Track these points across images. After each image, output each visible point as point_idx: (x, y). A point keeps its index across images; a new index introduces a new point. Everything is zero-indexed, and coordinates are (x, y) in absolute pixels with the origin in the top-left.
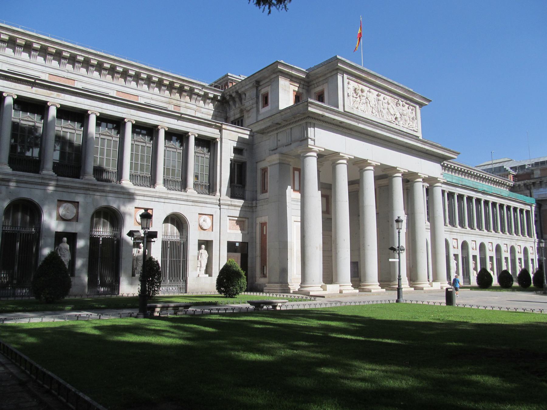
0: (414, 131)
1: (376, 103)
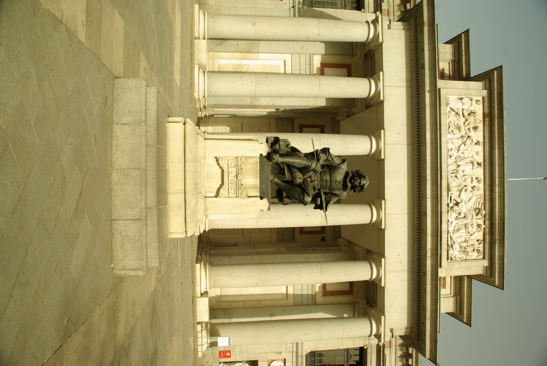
0: (448, 251)
1: (468, 160)
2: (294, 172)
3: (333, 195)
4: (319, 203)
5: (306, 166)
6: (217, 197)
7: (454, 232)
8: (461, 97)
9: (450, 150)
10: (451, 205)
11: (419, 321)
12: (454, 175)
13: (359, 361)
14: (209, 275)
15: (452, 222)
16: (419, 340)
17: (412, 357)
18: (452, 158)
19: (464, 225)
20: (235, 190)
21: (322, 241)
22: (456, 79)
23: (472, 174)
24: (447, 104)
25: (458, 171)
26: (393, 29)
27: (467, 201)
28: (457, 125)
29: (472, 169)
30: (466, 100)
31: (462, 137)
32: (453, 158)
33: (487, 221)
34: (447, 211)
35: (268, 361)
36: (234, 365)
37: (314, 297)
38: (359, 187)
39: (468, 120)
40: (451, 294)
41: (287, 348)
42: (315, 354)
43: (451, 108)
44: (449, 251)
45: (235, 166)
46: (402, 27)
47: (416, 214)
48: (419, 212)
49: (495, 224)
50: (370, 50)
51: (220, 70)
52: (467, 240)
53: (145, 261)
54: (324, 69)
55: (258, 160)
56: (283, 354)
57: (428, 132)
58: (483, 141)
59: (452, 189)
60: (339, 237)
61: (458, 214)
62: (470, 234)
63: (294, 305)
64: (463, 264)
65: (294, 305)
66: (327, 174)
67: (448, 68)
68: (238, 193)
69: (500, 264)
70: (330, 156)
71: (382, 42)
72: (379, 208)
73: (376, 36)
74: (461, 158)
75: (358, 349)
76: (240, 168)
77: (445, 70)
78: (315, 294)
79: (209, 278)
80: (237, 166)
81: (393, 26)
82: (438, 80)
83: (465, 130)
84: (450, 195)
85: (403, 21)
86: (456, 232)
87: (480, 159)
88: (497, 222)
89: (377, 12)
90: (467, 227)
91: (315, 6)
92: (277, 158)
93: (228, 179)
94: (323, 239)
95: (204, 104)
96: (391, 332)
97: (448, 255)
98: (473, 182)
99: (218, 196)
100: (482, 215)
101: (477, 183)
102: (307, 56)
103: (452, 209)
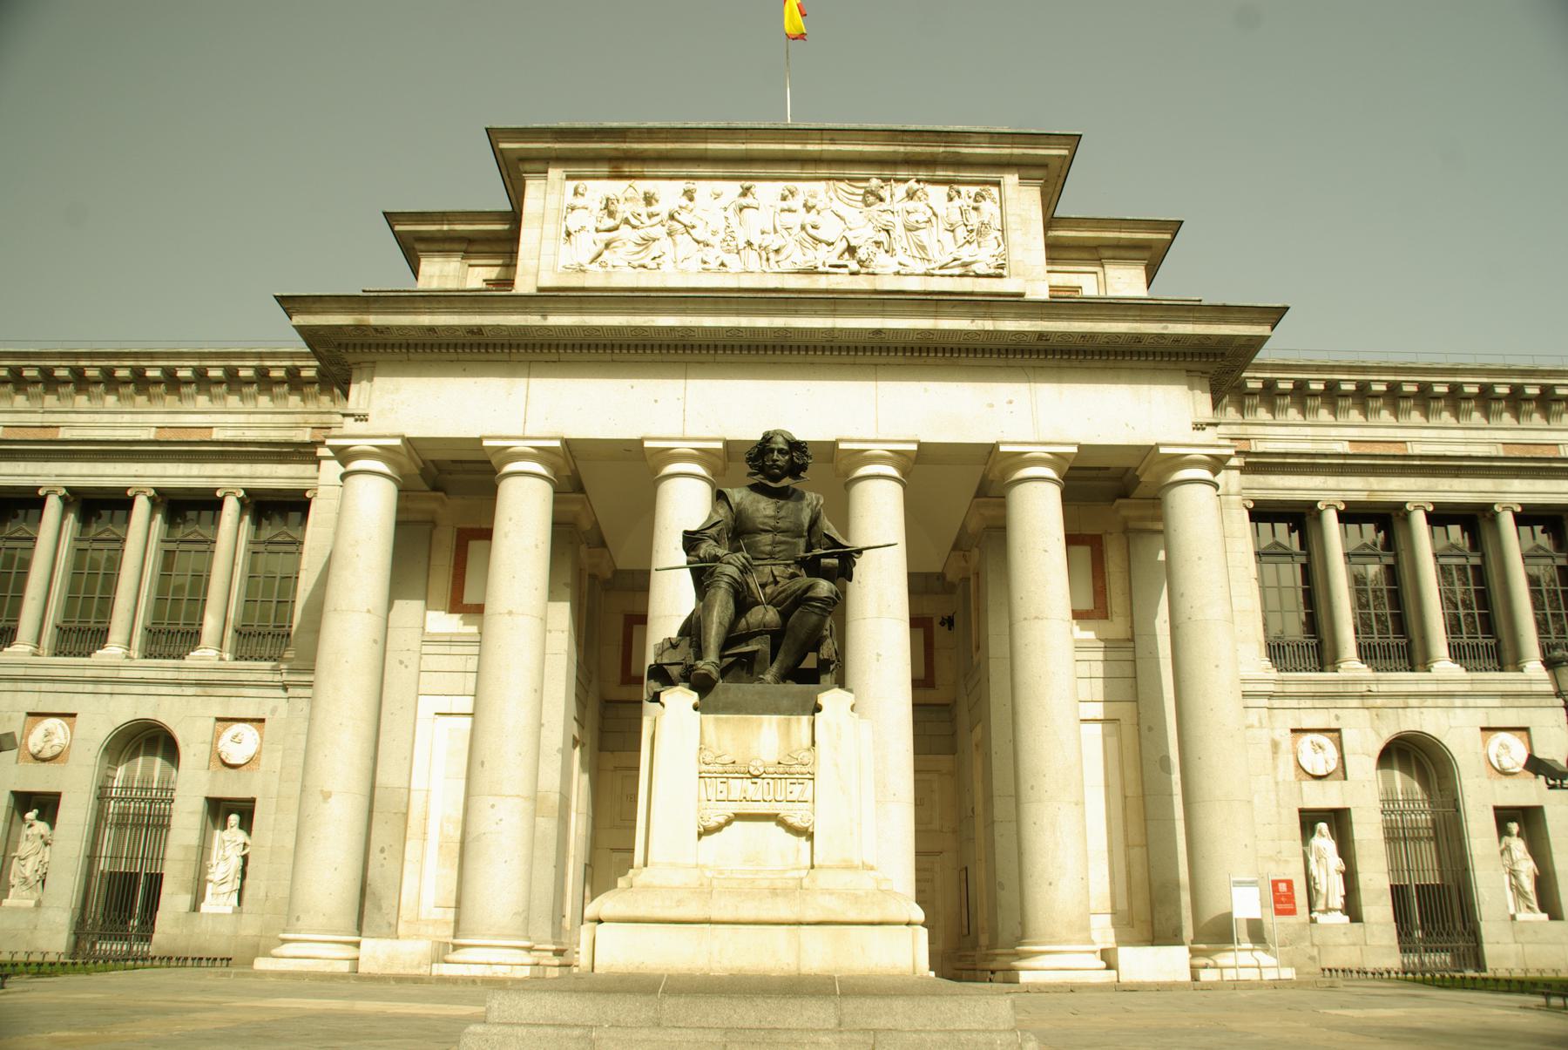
0: (978, 276)
1: (734, 221)
2: (748, 628)
3: (815, 528)
4: (836, 561)
5: (732, 590)
6: (813, 833)
7: (928, 260)
8: (564, 235)
9: (706, 266)
10: (854, 266)
11: (1170, 354)
12: (772, 255)
13: (1291, 524)
14: (1050, 943)
15: (901, 264)
16: (1223, 354)
17: (1273, 382)
19: (909, 233)
20: (795, 784)
21: (953, 625)
22: (515, 250)
23: (772, 210)
24: (580, 270)
25: (764, 245)
26: (368, 407)
27: (845, 223)
28: (639, 245)
29: (757, 209)
30: (573, 222)
31: (670, 234)
32: (727, 259)
33: (898, 173)
35: (1300, 780)
36: (1317, 881)
37: (1110, 645)
38: (794, 454)
39: (626, 218)
40: (1096, 273)
41: (1261, 722)
42: (1274, 647)
43: (592, 261)
44: (978, 272)
45: (725, 780)
46: (364, 384)
47: (877, 358)
48: (872, 349)
49: (906, 153)
50: (420, 475)
51: (453, 904)
52: (948, 227)
53: (994, 1036)
54: (467, 605)
55: (711, 717)
56: (1277, 738)
57: (653, 321)
58: (685, 181)
59: (812, 264)
60: (941, 576)
61: (879, 247)
62: (933, 218)
63: (1135, 699)
64: (1013, 236)
65: (1135, 699)
66: (754, 542)
67: (484, 268)
68: (802, 774)
69: (1013, 144)
70: (706, 531)
71: (402, 437)
72: (860, 457)
73: (385, 453)
74: (729, 238)
75: (1257, 526)
76: (730, 768)
77: (488, 277)
78: (1101, 640)
79: (1059, 943)
80: (725, 775)
81: (361, 407)
82: (513, 292)
83: (651, 226)
84: (827, 269)
85: (349, 383)
86: (926, 254)
88: (902, 149)
89: (318, 454)
90: (913, 226)
91: (287, 628)
92: (709, 663)
93: (762, 802)
94: (949, 622)
95: (551, 954)
96: (1204, 429)
97: (988, 276)
98: (794, 209)
99: (810, 830)
100: (882, 187)
101: (797, 197)
102: (426, 649)
103: (866, 264)
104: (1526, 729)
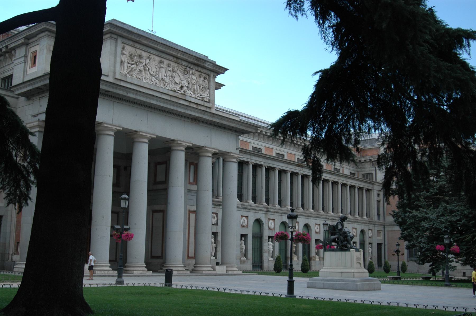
1: (158, 70)
18: (157, 82)
34: (184, 96)
44: (205, 100)
87: (158, 59)
88: (196, 62)
104: (247, 217)
